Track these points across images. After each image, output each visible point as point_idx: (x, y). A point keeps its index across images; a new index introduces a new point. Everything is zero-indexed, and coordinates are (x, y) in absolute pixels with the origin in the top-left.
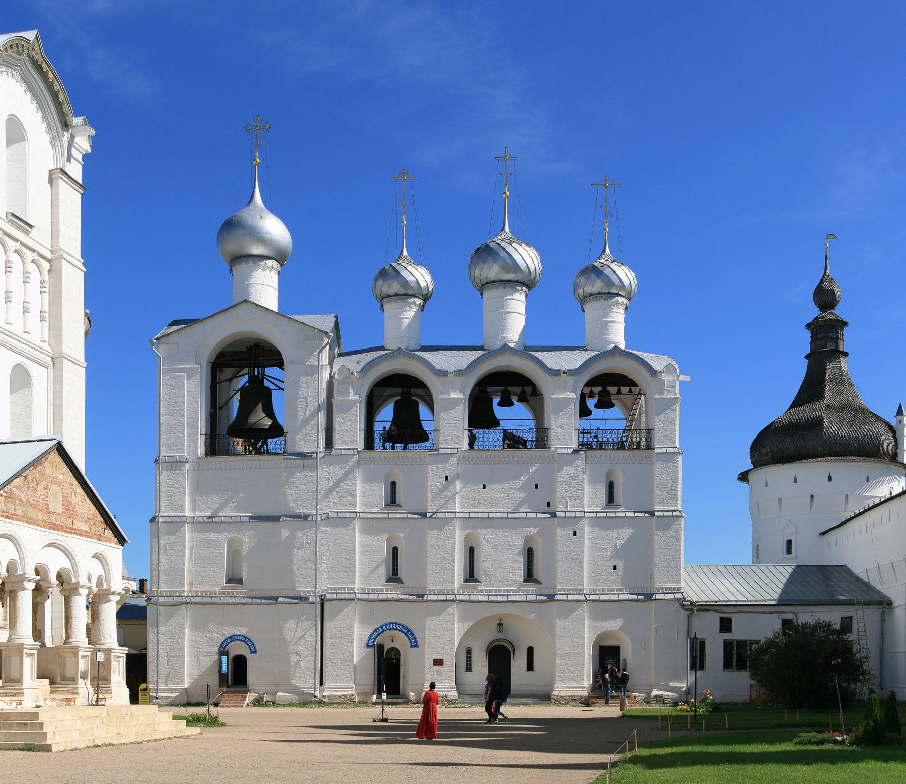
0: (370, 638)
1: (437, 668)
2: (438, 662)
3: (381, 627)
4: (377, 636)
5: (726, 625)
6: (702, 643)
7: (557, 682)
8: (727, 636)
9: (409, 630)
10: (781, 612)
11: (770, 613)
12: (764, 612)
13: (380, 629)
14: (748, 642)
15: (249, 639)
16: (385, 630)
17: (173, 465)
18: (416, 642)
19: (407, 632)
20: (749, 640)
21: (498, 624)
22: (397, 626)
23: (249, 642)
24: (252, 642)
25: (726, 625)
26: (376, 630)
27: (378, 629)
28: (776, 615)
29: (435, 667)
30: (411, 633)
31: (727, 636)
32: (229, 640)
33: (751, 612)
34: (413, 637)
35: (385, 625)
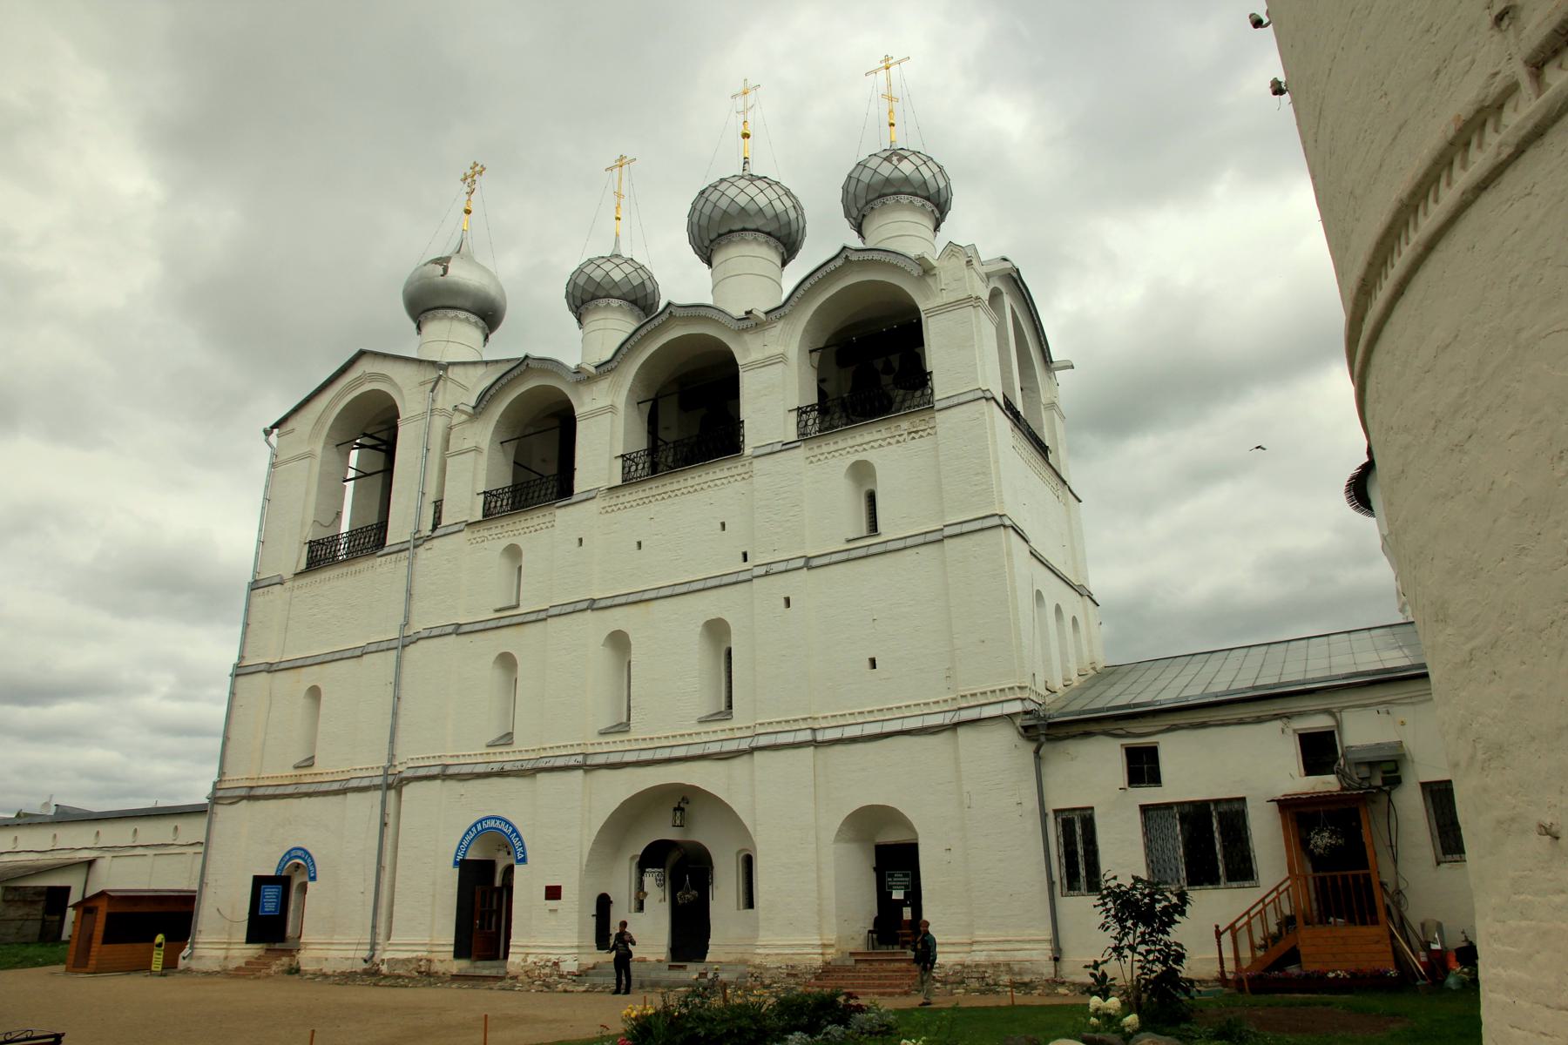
0: (459, 848)
1: (553, 904)
2: (553, 893)
3: (475, 825)
4: (469, 843)
5: (1143, 767)
6: (1087, 819)
7: (761, 933)
8: (1150, 795)
9: (514, 830)
10: (1288, 717)
11: (1259, 720)
12: (1241, 722)
13: (474, 829)
14: (1212, 807)
15: (310, 856)
16: (481, 831)
17: (266, 589)
18: (523, 853)
19: (512, 832)
20: (1217, 802)
21: (675, 809)
22: (498, 822)
23: (309, 860)
24: (312, 861)
25: (1143, 767)
26: (467, 833)
27: (470, 830)
28: (1277, 725)
29: (548, 901)
30: (518, 836)
31: (1150, 795)
32: (288, 857)
33: (1204, 725)
34: (519, 844)
35: (480, 822)
